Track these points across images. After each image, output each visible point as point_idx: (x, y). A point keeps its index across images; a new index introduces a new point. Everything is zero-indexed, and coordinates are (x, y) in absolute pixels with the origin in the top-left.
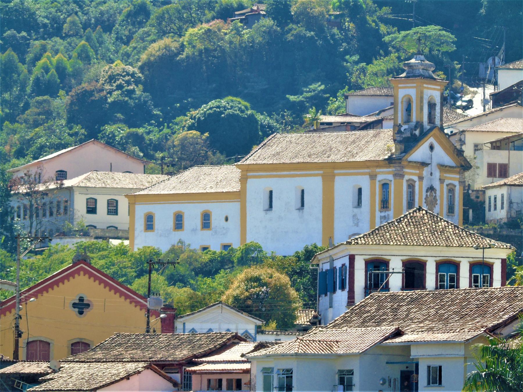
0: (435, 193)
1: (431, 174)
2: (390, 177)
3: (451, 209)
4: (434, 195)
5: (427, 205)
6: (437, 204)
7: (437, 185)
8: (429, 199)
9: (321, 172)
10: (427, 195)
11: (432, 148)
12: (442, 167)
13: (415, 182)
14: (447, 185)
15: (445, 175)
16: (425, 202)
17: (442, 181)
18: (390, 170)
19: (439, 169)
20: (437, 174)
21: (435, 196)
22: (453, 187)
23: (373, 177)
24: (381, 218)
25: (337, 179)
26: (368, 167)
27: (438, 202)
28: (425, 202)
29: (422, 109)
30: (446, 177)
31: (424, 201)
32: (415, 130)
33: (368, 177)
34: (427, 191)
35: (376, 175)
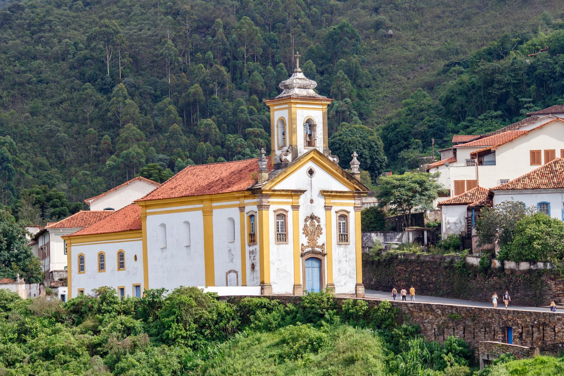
0: (319, 222)
1: (312, 201)
2: (255, 208)
3: (344, 238)
4: (317, 224)
7: (320, 212)
8: (310, 228)
9: (201, 206)
10: (306, 226)
11: (311, 172)
12: (326, 194)
15: (333, 201)
17: (328, 208)
18: (255, 200)
21: (319, 226)
23: (242, 209)
24: (250, 253)
25: (215, 212)
26: (238, 198)
27: (324, 231)
29: (293, 131)
30: (334, 203)
31: (301, 231)
32: (286, 155)
33: (237, 209)
34: (306, 220)
35: (244, 207)
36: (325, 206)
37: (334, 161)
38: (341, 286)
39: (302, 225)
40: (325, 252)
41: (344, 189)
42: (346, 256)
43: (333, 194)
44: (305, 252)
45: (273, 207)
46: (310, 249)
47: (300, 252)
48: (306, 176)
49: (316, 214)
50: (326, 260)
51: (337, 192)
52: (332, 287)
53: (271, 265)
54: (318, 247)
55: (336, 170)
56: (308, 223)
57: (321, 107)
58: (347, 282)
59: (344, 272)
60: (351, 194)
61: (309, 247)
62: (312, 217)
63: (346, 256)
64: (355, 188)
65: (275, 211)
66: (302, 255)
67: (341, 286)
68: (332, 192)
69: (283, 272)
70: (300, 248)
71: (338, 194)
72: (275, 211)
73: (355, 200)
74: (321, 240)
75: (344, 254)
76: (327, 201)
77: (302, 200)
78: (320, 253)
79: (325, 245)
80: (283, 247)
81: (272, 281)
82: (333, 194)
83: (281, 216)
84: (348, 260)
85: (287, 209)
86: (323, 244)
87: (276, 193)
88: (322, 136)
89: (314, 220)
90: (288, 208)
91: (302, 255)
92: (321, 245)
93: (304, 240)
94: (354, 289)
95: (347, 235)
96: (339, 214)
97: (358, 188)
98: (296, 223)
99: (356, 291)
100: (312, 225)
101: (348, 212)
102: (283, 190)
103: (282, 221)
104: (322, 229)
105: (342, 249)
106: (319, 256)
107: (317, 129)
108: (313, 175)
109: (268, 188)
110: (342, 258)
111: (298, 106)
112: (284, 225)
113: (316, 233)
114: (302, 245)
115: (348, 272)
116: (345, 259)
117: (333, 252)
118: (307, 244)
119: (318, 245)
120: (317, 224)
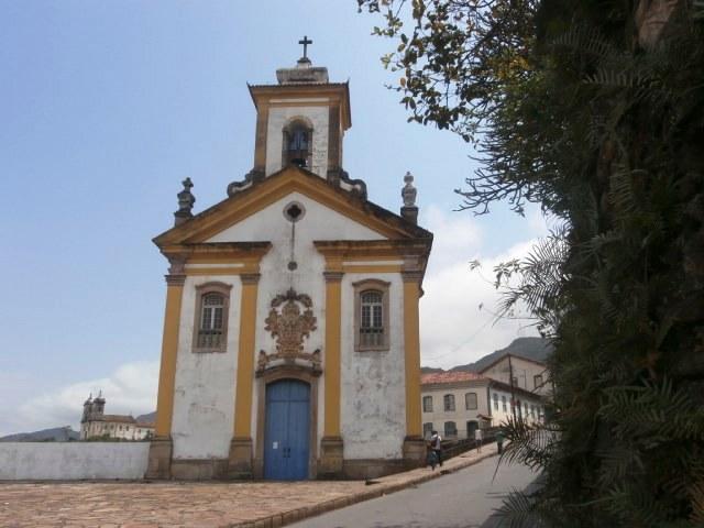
1: (293, 266)
4: (303, 310)
6: (314, 329)
10: (273, 313)
11: (294, 212)
13: (229, 287)
14: (354, 285)
15: (345, 264)
16: (267, 329)
17: (333, 277)
19: (320, 252)
20: (319, 264)
21: (309, 313)
22: (378, 287)
27: (321, 323)
28: (267, 329)
31: (261, 323)
34: (275, 303)
36: (325, 274)
37: (354, 190)
38: (362, 442)
40: (323, 365)
41: (382, 238)
42: (379, 376)
43: (340, 247)
44: (267, 367)
45: (191, 282)
46: (281, 361)
47: (256, 366)
48: (286, 223)
49: (300, 289)
51: (349, 243)
52: (335, 443)
53: (177, 396)
54: (305, 357)
55: (349, 202)
56: (280, 309)
57: (326, 100)
58: (380, 432)
59: (372, 411)
60: (389, 247)
61: (277, 357)
62: (291, 296)
63: (379, 376)
64: (401, 234)
65: (198, 288)
66: (260, 374)
67: (362, 442)
68: (336, 243)
69: (206, 412)
70: (257, 358)
71: (355, 248)
72: (198, 288)
73: (404, 259)
74: (313, 341)
75: (374, 371)
76: (331, 264)
77: (266, 265)
78: (303, 369)
79: (323, 352)
80: (211, 359)
81: (175, 429)
82: (340, 247)
83: (213, 297)
84: (381, 383)
85: (229, 283)
86: (317, 352)
87: (197, 251)
88: (326, 148)
89: (296, 302)
90: (234, 280)
92: (311, 351)
93: (267, 343)
94: (399, 450)
96: (359, 290)
97: (405, 233)
98: (250, 312)
101: (387, 284)
102: (213, 245)
104: (315, 320)
105: (368, 360)
106: (305, 377)
107: (314, 137)
109: (179, 241)
110: (367, 380)
111: (272, 101)
112: (222, 317)
114: (262, 352)
115: (383, 411)
116: (376, 381)
117: (344, 368)
118: (276, 352)
119: (305, 351)
120: (303, 310)
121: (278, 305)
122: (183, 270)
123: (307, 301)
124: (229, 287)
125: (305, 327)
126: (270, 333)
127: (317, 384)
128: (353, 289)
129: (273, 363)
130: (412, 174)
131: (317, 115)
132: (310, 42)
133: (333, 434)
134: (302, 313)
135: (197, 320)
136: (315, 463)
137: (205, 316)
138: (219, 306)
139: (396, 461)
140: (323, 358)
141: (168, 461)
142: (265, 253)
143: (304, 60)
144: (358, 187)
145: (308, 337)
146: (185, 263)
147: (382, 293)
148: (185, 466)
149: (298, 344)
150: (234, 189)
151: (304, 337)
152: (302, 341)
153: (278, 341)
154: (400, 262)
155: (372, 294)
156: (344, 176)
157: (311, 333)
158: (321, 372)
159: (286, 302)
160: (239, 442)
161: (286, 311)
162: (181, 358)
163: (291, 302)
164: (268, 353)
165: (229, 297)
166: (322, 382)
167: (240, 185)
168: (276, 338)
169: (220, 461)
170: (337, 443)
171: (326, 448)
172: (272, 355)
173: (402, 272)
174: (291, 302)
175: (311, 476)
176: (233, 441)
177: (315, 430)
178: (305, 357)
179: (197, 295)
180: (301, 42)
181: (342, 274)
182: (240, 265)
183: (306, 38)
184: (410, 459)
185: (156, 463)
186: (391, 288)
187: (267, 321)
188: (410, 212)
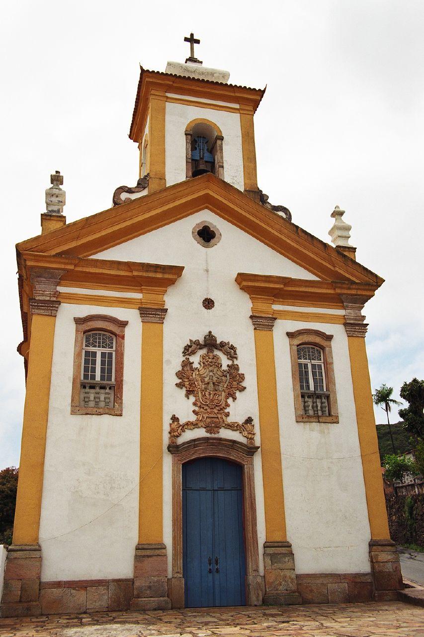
1: (208, 304)
4: (225, 362)
5: (189, 393)
10: (187, 364)
11: (206, 235)
13: (124, 324)
15: (277, 307)
16: (179, 386)
17: (262, 323)
21: (234, 368)
22: (318, 340)
27: (250, 382)
31: (170, 379)
34: (189, 350)
36: (251, 317)
39: (173, 362)
45: (68, 313)
46: (201, 433)
47: (166, 439)
49: (221, 337)
50: (257, 468)
52: (281, 550)
54: (232, 427)
57: (237, 106)
70: (166, 428)
72: (78, 321)
73: (344, 308)
74: (243, 407)
79: (256, 422)
83: (100, 334)
86: (249, 420)
89: (217, 353)
91: (173, 448)
92: (241, 420)
93: (180, 405)
95: (328, 397)
96: (297, 341)
99: (373, 561)
100: (211, 363)
101: (329, 338)
103: (107, 350)
104: (242, 377)
108: (212, 241)
109: (53, 253)
113: (223, 386)
114: (174, 419)
118: (193, 418)
120: (225, 362)
121: (193, 353)
122: (58, 294)
123: (231, 351)
124: (124, 324)
125: (230, 386)
126: (183, 392)
127: (252, 464)
128: (287, 340)
129: (189, 435)
130: (341, 209)
131: (226, 122)
132: (198, 42)
133: (277, 537)
134: (225, 367)
135: (77, 366)
136: (259, 580)
137: (87, 362)
138: (107, 350)
139: (354, 579)
140: (257, 430)
141: (37, 587)
142: (172, 282)
143: (192, 59)
144: (281, 214)
145: (234, 399)
146: (58, 284)
147: (323, 348)
148: (56, 591)
149: (222, 409)
150: (124, 196)
151: (230, 401)
152: (228, 405)
153: (195, 404)
154: (342, 312)
155: (311, 347)
156: (263, 198)
157: (238, 394)
158: (259, 447)
159: (204, 352)
160: (146, 551)
161: (205, 363)
162: (55, 420)
163: (210, 351)
164: (182, 421)
165: (123, 337)
166: (257, 460)
167: (130, 191)
168: (192, 399)
169: (118, 581)
170: (283, 550)
171: (273, 557)
172: (187, 424)
173: (345, 324)
174: (210, 351)
175: (253, 599)
176: (137, 549)
177: (255, 532)
178: (232, 427)
179: (77, 331)
180: (186, 39)
181: (275, 319)
182: (139, 296)
183: (192, 35)
184: (380, 572)
185: (16, 586)
186: (333, 343)
187: (179, 375)
188: (345, 254)
